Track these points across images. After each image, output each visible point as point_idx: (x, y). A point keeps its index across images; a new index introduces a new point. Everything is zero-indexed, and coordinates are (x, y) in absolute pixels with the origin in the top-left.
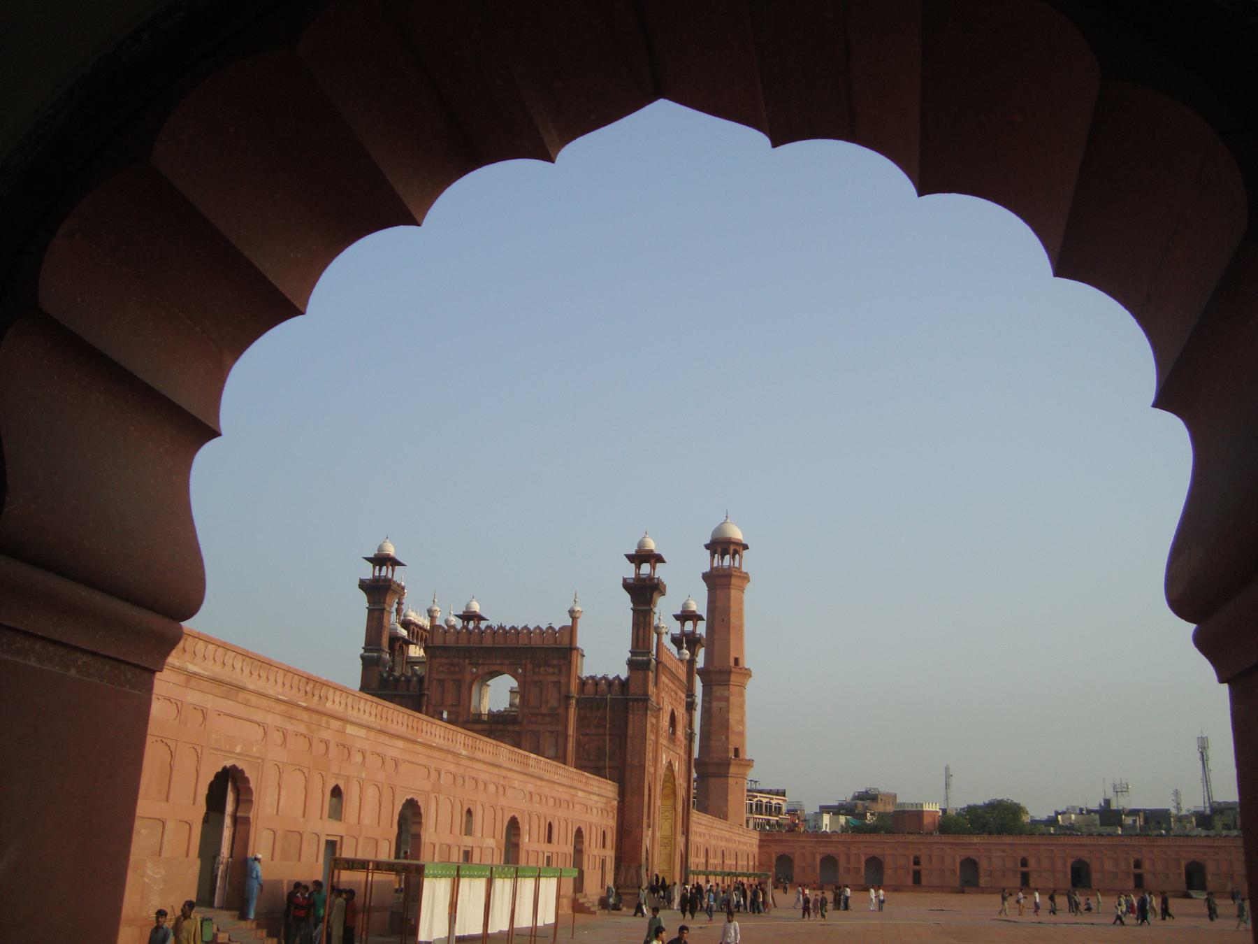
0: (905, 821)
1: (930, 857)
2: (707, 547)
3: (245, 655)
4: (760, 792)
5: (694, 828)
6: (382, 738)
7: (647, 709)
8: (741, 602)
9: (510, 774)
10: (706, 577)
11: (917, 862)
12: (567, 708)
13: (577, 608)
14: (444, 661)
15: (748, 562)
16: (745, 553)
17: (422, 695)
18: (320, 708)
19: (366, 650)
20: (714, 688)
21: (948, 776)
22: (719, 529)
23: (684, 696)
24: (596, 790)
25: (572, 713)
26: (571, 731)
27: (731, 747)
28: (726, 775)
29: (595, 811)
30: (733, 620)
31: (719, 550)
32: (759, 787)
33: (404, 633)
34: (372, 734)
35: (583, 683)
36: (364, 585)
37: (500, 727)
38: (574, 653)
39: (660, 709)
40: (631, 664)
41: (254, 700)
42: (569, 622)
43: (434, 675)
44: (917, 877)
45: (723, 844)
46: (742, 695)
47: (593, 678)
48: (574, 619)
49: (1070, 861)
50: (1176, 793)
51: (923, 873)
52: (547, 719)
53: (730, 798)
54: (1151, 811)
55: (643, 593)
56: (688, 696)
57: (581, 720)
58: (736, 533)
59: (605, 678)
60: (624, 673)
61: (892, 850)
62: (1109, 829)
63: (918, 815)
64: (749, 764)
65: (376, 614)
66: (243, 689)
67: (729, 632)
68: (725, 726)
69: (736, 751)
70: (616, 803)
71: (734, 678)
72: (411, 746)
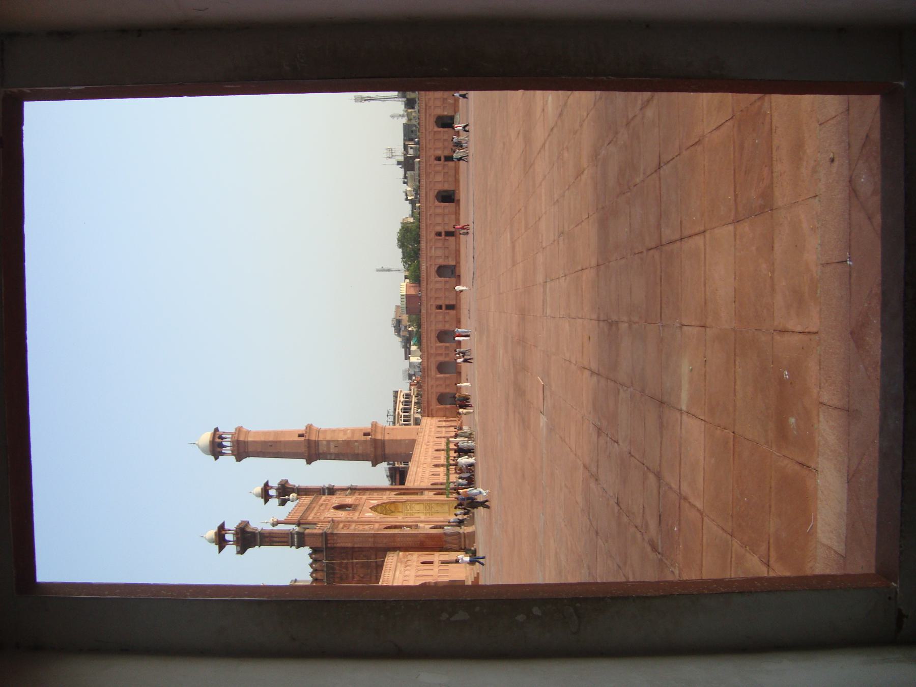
0: (412, 305)
1: (436, 298)
2: (216, 458)
4: (395, 410)
5: (417, 485)
8: (257, 433)
10: (239, 459)
11: (440, 307)
15: (228, 428)
16: (221, 430)
20: (321, 451)
21: (383, 270)
22: (204, 451)
23: (324, 497)
24: (391, 573)
28: (383, 442)
29: (407, 573)
30: (271, 439)
31: (219, 449)
32: (392, 410)
35: (315, 580)
39: (333, 521)
40: (301, 545)
44: (450, 307)
45: (431, 450)
46: (325, 431)
47: (311, 575)
49: (437, 203)
50: (393, 116)
51: (447, 303)
54: (405, 135)
56: (324, 494)
58: (206, 438)
59: (311, 565)
60: (307, 550)
61: (435, 322)
62: (416, 167)
63: (409, 297)
64: (374, 425)
68: (347, 443)
69: (366, 434)
70: (401, 553)
71: (313, 438)
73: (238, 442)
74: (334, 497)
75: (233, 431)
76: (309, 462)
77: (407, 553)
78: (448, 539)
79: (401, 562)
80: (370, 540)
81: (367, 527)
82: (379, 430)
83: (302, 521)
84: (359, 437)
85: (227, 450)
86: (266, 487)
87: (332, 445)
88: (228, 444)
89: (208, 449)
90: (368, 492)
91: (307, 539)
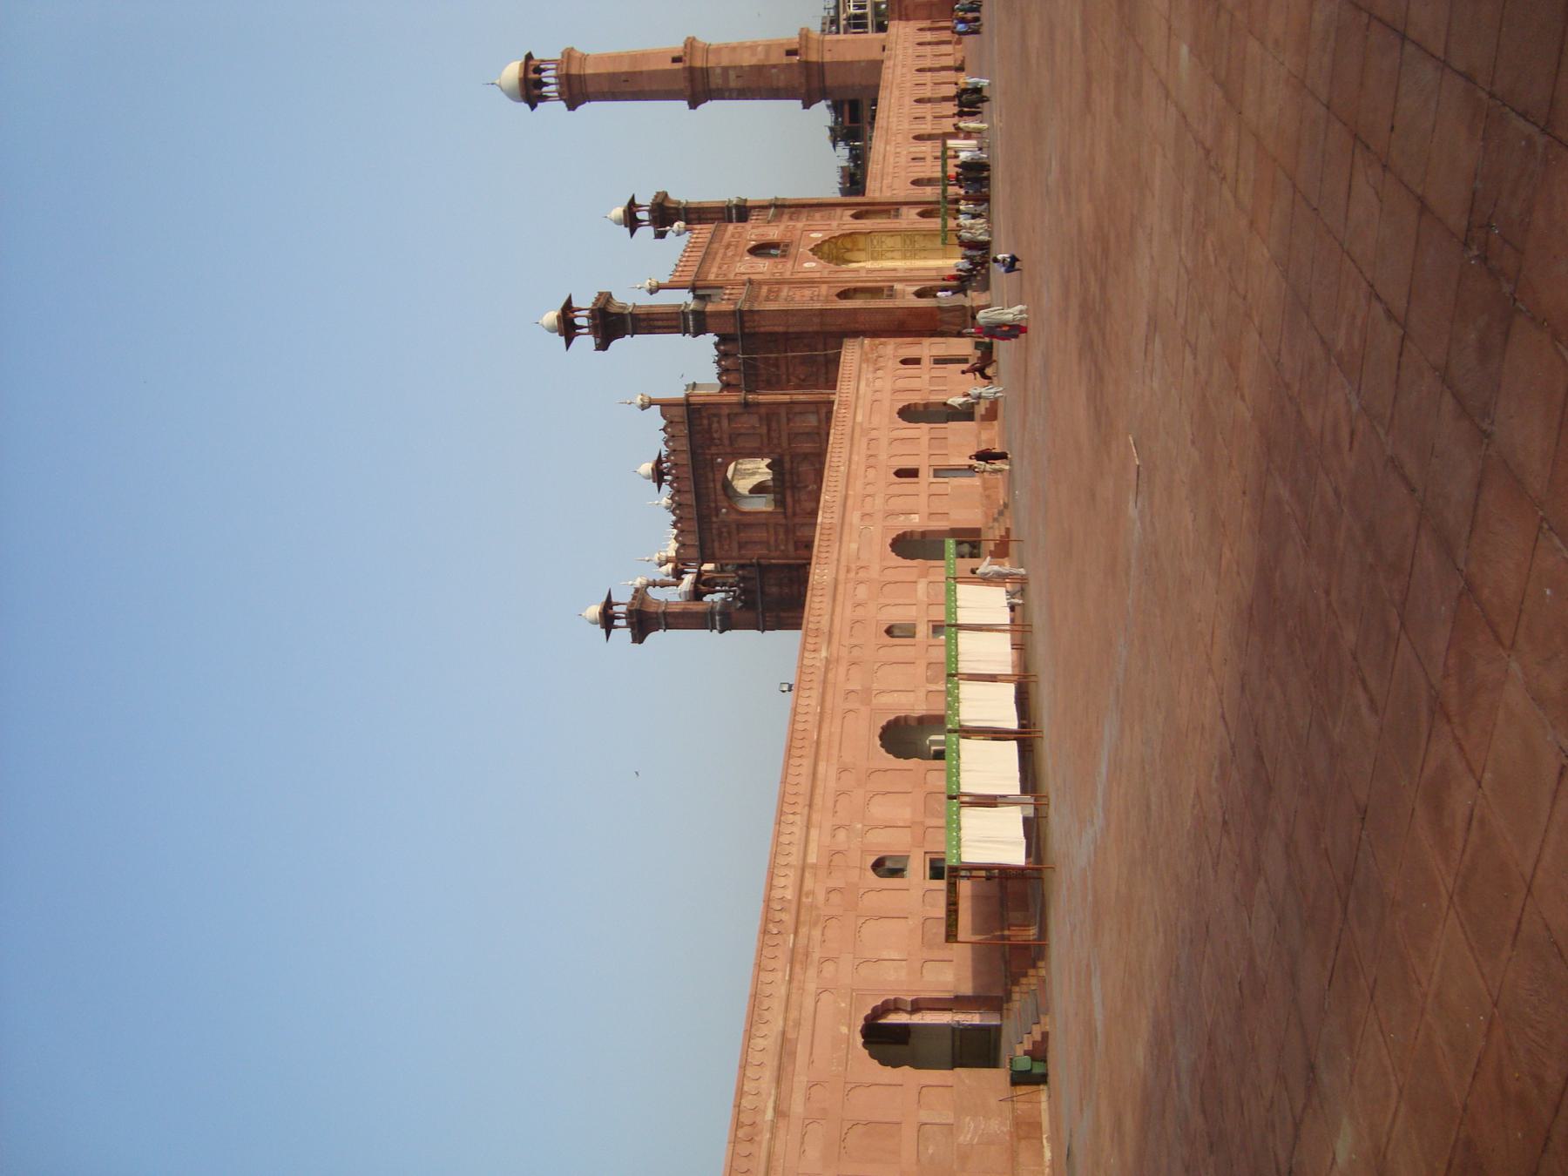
2: (533, 107)
3: (749, 1036)
6: (818, 800)
7: (751, 311)
9: (843, 562)
10: (572, 106)
12: (758, 404)
13: (638, 401)
14: (716, 544)
15: (547, 52)
16: (537, 56)
17: (759, 565)
18: (794, 907)
19: (713, 628)
20: (713, 86)
22: (511, 95)
23: (731, 227)
24: (853, 384)
25: (765, 397)
26: (786, 398)
27: (785, 60)
29: (878, 384)
30: (625, 68)
31: (536, 92)
33: (688, 579)
34: (816, 817)
35: (727, 386)
36: (639, 637)
37: (787, 477)
38: (692, 400)
39: (751, 282)
40: (700, 330)
41: (793, 1014)
42: (656, 409)
43: (735, 554)
45: (908, 101)
46: (719, 50)
47: (720, 376)
48: (651, 403)
52: (774, 425)
53: (848, 59)
55: (610, 324)
56: (730, 221)
57: (771, 385)
58: (512, 71)
60: (710, 338)
65: (670, 620)
66: (784, 1033)
67: (641, 73)
68: (759, 70)
69: (790, 53)
70: (867, 341)
71: (698, 63)
72: (823, 747)
73: (568, 77)
74: (748, 226)
75: (559, 57)
76: (693, 105)
77: (877, 341)
78: (947, 317)
79: (867, 360)
80: (816, 320)
81: (807, 293)
82: (813, 45)
83: (699, 283)
84: (778, 58)
85: (550, 90)
86: (632, 207)
87: (732, 74)
88: (552, 80)
89: (518, 91)
90: (805, 210)
91: (709, 321)
